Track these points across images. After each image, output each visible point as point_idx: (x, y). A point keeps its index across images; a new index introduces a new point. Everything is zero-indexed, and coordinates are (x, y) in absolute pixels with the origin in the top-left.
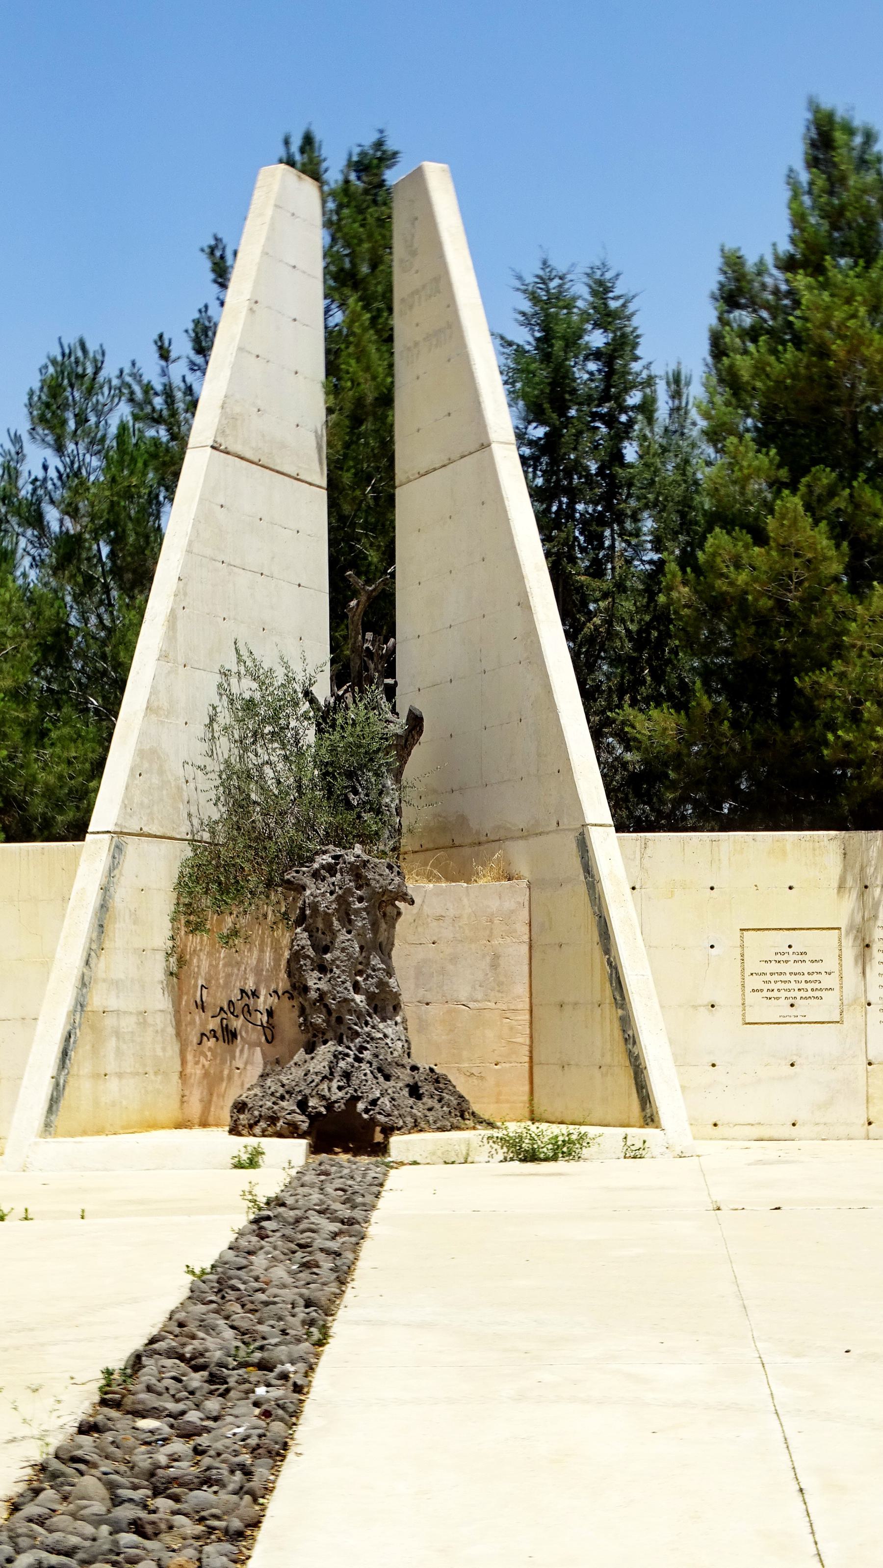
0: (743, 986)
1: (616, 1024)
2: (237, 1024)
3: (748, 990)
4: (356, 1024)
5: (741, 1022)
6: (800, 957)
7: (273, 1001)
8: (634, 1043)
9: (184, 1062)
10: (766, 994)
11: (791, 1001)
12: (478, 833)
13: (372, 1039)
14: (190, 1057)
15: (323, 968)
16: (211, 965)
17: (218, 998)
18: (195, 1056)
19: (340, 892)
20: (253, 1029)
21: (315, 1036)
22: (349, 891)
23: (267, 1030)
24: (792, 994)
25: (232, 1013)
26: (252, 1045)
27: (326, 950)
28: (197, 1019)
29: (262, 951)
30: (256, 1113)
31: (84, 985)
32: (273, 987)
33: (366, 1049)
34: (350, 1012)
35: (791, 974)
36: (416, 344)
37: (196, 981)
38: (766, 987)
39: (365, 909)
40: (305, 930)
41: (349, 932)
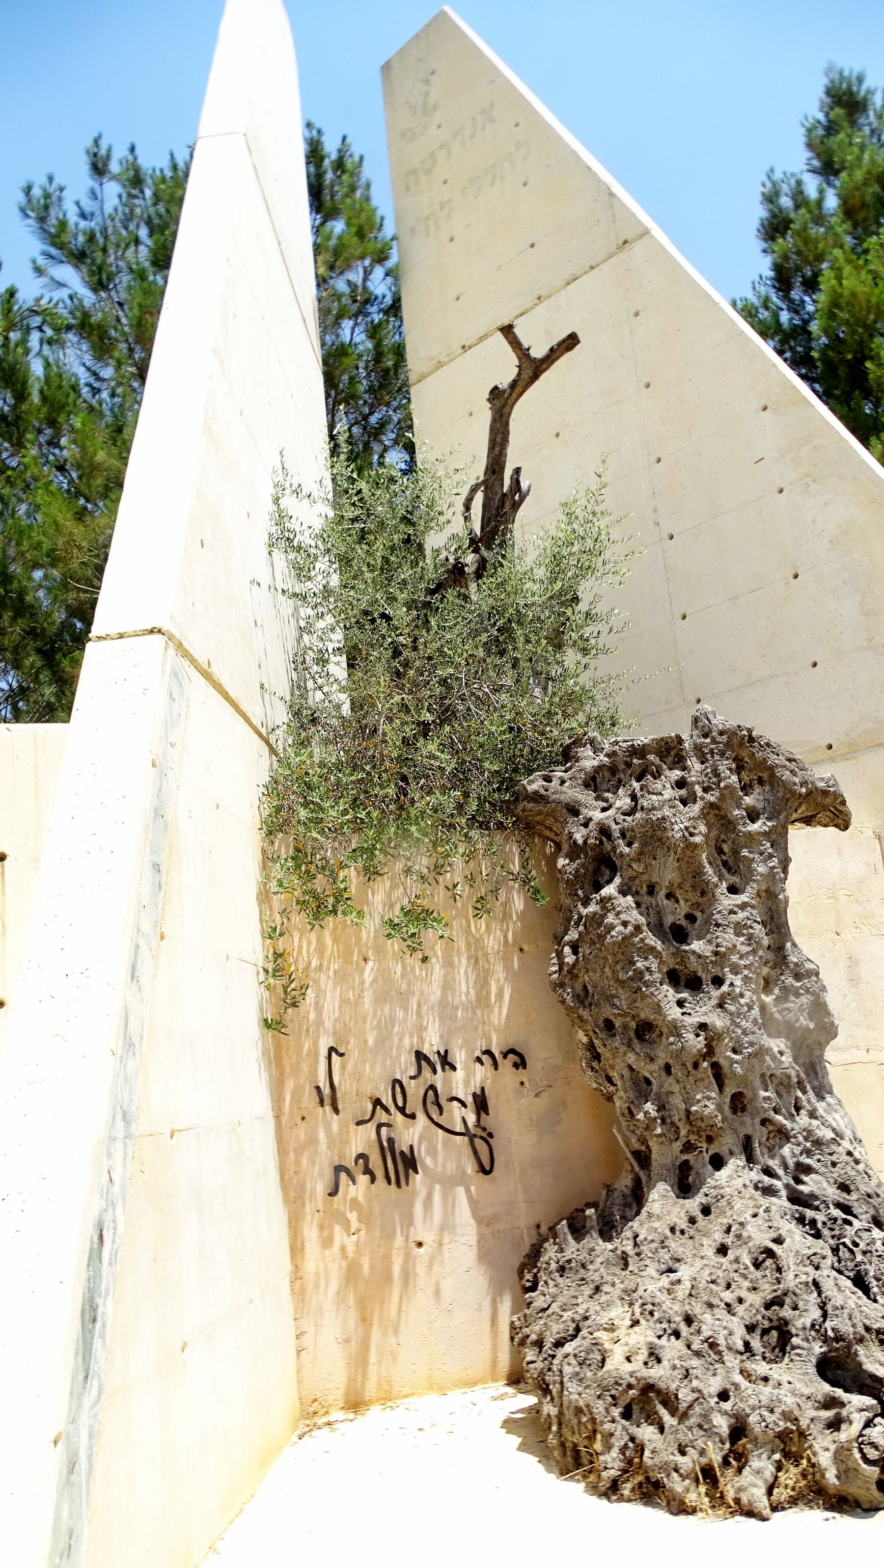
2: (411, 1134)
4: (776, 1111)
7: (481, 1074)
9: (296, 1249)
13: (818, 1143)
14: (311, 1233)
15: (687, 981)
16: (344, 1001)
17: (365, 1076)
18: (321, 1227)
19: (711, 798)
20: (445, 1143)
21: (688, 1147)
22: (727, 793)
23: (477, 1141)
25: (402, 1110)
26: (449, 1183)
27: (679, 935)
28: (322, 1135)
29: (449, 964)
30: (722, 1424)
32: (480, 1045)
33: (808, 1170)
34: (766, 1079)
37: (316, 1044)
39: (765, 834)
40: (623, 892)
41: (733, 890)
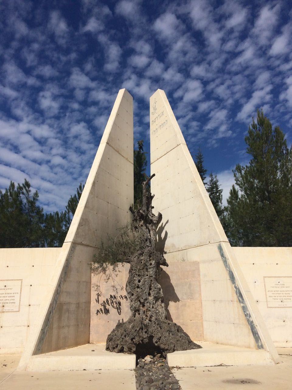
0: (266, 295)
1: (241, 309)
3: (268, 296)
5: (267, 307)
6: (282, 286)
8: (250, 316)
10: (273, 298)
11: (282, 300)
12: (178, 248)
24: (281, 298)
31: (58, 293)
35: (280, 291)
36: (157, 129)
38: (273, 295)
